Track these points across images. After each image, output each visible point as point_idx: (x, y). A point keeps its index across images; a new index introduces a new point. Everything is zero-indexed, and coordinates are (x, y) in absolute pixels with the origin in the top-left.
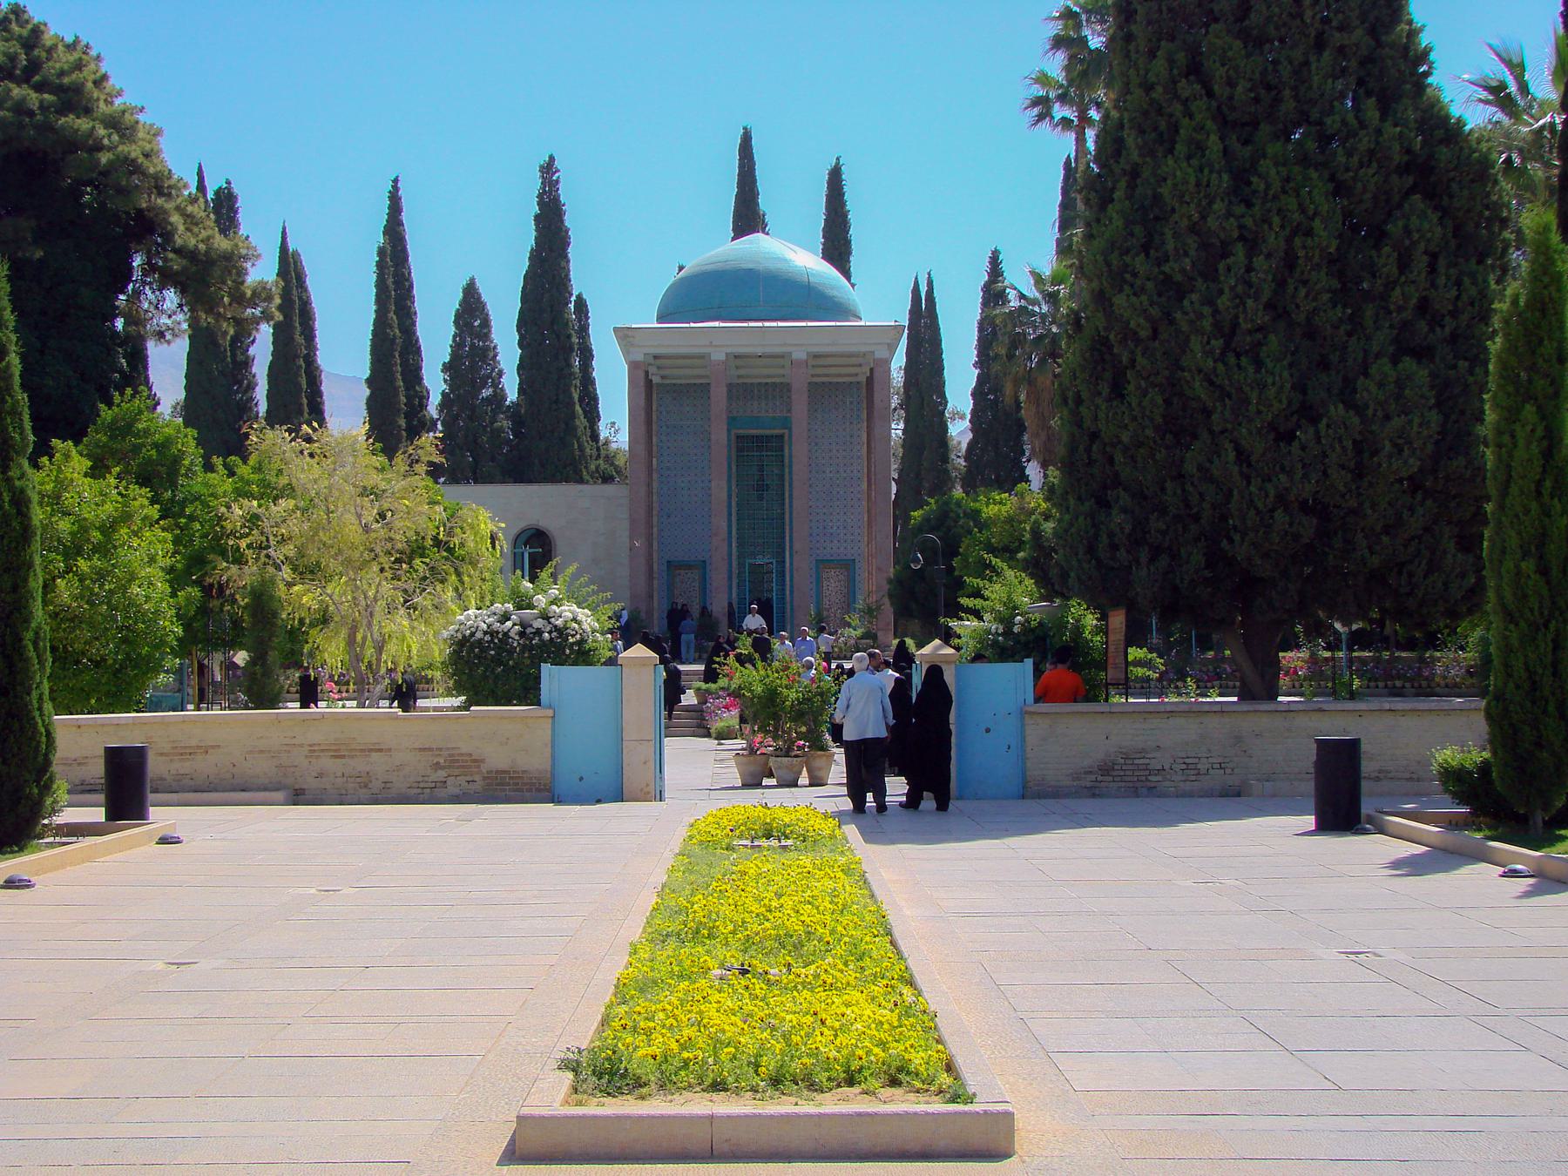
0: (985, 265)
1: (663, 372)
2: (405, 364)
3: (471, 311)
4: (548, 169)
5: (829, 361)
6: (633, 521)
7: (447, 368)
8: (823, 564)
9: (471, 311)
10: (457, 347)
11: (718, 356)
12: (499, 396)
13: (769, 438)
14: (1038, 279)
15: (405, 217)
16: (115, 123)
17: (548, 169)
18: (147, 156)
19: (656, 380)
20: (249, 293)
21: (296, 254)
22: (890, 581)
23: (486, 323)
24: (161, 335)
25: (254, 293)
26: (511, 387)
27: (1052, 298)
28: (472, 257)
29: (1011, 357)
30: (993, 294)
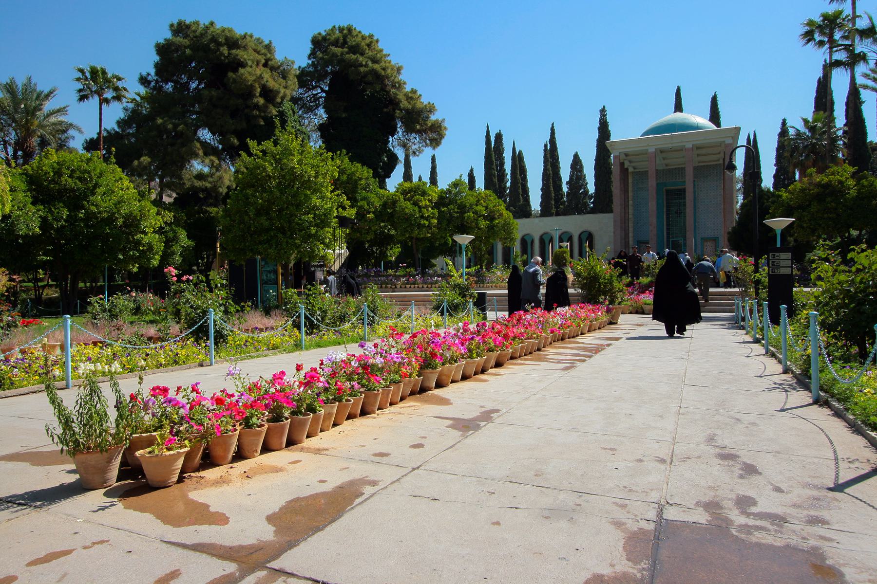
0: (780, 125)
1: (633, 164)
2: (554, 182)
3: (577, 164)
4: (603, 111)
5: (704, 151)
6: (615, 221)
7: (567, 183)
8: (705, 240)
9: (577, 164)
10: (571, 177)
11: (652, 150)
12: (586, 192)
13: (680, 190)
14: (806, 121)
15: (556, 136)
16: (375, 61)
17: (603, 111)
18: (384, 69)
19: (631, 170)
20: (430, 124)
21: (520, 152)
22: (729, 233)
23: (582, 167)
24: (414, 153)
25: (432, 125)
26: (591, 189)
27: (812, 129)
28: (579, 146)
29: (792, 156)
30: (784, 132)
